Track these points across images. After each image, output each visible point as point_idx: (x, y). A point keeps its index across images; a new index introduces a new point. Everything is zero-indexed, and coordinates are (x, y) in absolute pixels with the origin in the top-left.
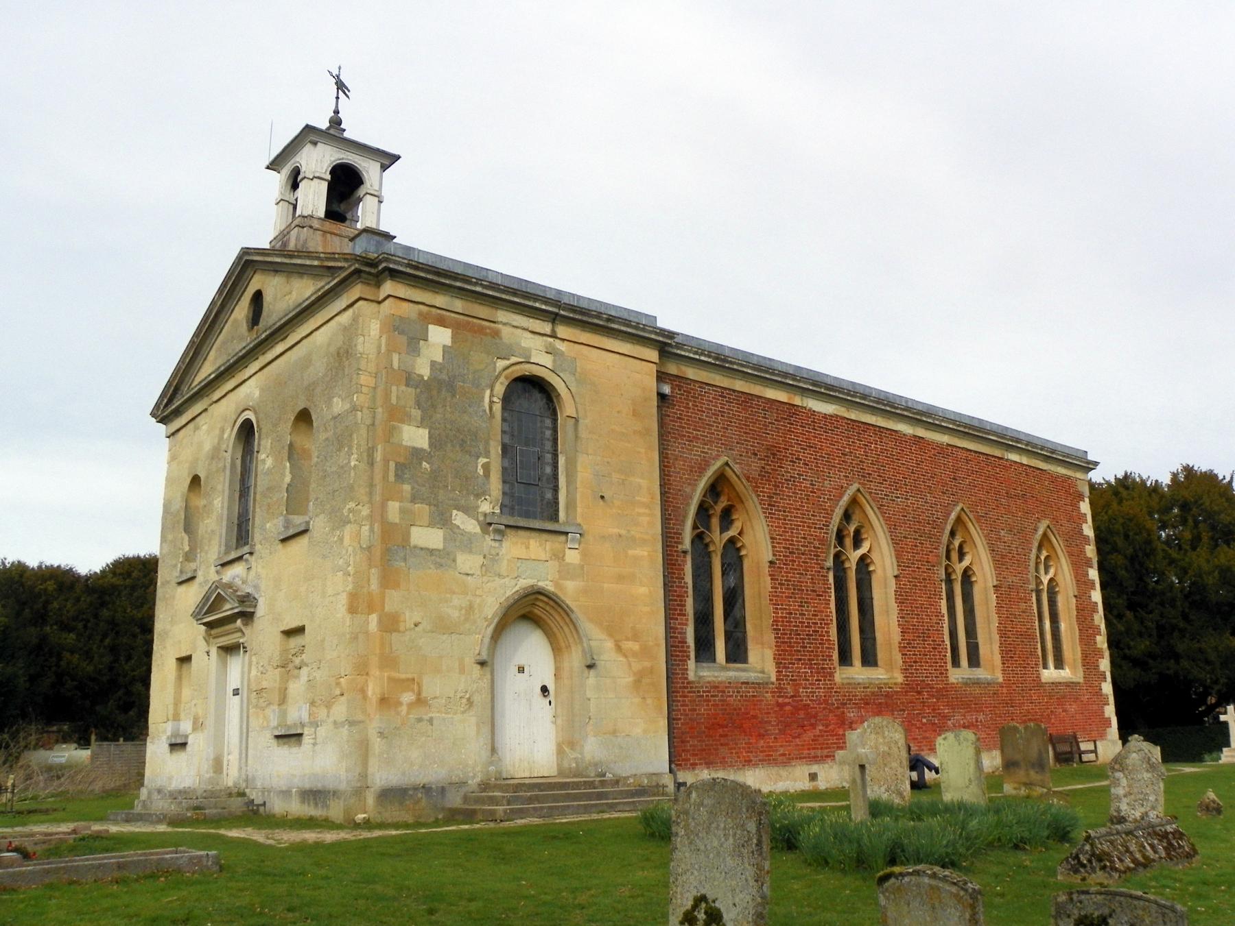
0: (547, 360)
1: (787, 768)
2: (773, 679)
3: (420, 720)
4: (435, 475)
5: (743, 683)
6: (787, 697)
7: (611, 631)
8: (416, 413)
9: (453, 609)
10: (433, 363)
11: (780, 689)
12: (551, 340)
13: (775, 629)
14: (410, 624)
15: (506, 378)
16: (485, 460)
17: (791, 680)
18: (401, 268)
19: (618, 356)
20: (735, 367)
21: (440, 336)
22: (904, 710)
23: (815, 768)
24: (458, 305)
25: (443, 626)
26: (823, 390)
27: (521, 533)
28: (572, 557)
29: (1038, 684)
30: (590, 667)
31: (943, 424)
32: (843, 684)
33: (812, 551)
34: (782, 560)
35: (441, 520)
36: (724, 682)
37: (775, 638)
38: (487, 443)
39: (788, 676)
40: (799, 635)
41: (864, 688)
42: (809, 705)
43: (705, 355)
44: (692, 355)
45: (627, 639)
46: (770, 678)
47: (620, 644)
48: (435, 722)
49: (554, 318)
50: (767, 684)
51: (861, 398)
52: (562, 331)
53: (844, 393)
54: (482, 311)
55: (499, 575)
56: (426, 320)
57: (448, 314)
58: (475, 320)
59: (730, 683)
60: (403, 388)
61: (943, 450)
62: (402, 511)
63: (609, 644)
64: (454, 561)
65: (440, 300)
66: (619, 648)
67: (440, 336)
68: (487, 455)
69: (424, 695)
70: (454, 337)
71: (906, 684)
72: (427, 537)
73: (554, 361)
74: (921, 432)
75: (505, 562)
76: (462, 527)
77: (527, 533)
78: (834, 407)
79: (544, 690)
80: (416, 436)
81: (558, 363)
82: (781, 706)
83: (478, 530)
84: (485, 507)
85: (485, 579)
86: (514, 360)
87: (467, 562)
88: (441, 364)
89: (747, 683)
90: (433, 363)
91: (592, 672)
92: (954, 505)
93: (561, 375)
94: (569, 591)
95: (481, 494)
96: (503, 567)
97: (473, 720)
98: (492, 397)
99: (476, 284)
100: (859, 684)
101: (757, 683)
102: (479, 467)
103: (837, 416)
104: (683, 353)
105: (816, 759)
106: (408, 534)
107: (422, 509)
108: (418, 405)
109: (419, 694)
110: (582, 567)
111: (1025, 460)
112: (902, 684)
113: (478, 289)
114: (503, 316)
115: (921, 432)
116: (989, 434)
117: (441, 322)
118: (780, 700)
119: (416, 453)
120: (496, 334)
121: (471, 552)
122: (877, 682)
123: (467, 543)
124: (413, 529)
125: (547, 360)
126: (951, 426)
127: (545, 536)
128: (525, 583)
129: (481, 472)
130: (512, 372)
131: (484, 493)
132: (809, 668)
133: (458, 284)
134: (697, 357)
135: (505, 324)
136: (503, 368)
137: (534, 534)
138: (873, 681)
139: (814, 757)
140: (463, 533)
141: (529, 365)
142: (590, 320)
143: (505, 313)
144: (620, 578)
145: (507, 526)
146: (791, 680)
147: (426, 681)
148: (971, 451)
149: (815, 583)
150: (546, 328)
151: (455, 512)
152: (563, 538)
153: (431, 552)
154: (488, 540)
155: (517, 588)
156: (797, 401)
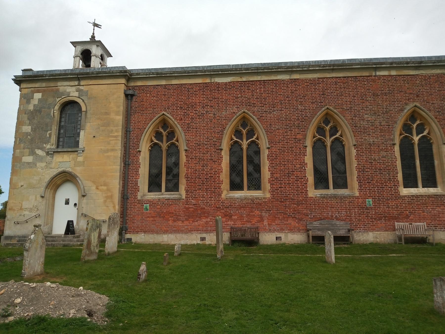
1: (187, 234)
2: (184, 197)
3: (20, 215)
5: (166, 200)
6: (191, 205)
8: (28, 122)
10: (34, 105)
11: (187, 202)
12: (79, 87)
13: (186, 177)
14: (20, 186)
15: (59, 104)
16: (50, 132)
17: (194, 198)
18: (21, 79)
19: (107, 85)
20: (168, 75)
21: (38, 96)
22: (271, 211)
23: (204, 235)
24: (44, 85)
25: (31, 186)
26: (220, 73)
27: (61, 153)
29: (398, 197)
30: (84, 196)
31: (311, 69)
32: (227, 199)
33: (211, 143)
34: (193, 149)
35: (32, 153)
36: (156, 200)
37: (186, 181)
38: (51, 126)
39: (193, 196)
40: (201, 179)
41: (241, 200)
42: (204, 208)
43: (151, 74)
44: (145, 76)
45: (101, 186)
46: (182, 197)
47: (98, 187)
48: (25, 216)
49: (79, 79)
50: (180, 199)
51: (245, 70)
52: (82, 83)
53: (233, 71)
54: (52, 84)
55: (51, 168)
56: (33, 92)
57: (41, 88)
58: (50, 88)
59: (159, 200)
60: (24, 115)
61: (313, 82)
64: (36, 165)
65: (37, 85)
67: (38, 96)
68: (51, 130)
70: (42, 96)
71: (272, 198)
72: (28, 159)
73: (79, 94)
74: (296, 76)
75: (54, 163)
76: (39, 154)
77: (63, 153)
80: (27, 129)
81: (81, 94)
83: (45, 154)
84: (48, 146)
85: (46, 170)
86: (63, 97)
88: (37, 105)
89: (169, 200)
90: (34, 105)
91: (85, 198)
92: (321, 108)
93: (82, 98)
94: (78, 171)
95: (47, 142)
96: (53, 165)
98: (56, 111)
99: (46, 76)
100: (238, 198)
101: (174, 200)
102: (48, 134)
103: (234, 82)
104: (141, 76)
106: (21, 159)
108: (28, 119)
109: (21, 207)
111: (394, 73)
112: (269, 198)
113: (47, 78)
114: (59, 84)
115: (296, 76)
116: (352, 66)
117: (38, 92)
118: (187, 206)
119: (27, 134)
120: (58, 90)
121: (42, 162)
122: (250, 197)
123: (41, 159)
124: (23, 158)
125: (77, 94)
126: (317, 68)
127: (70, 153)
128: (60, 170)
129: (48, 136)
130: (62, 101)
131: (49, 142)
132: (205, 192)
133: (40, 78)
134: (148, 76)
135: (61, 86)
136: (59, 101)
137: (65, 153)
138: (248, 197)
139: (205, 230)
140: (40, 156)
141: (69, 97)
142: (90, 76)
143: (60, 82)
145: (54, 152)
146: (194, 198)
148: (340, 77)
149: (213, 156)
150: (76, 83)
151: (36, 150)
152: (76, 153)
153: (28, 163)
154: (49, 158)
155: (58, 172)
156: (208, 81)
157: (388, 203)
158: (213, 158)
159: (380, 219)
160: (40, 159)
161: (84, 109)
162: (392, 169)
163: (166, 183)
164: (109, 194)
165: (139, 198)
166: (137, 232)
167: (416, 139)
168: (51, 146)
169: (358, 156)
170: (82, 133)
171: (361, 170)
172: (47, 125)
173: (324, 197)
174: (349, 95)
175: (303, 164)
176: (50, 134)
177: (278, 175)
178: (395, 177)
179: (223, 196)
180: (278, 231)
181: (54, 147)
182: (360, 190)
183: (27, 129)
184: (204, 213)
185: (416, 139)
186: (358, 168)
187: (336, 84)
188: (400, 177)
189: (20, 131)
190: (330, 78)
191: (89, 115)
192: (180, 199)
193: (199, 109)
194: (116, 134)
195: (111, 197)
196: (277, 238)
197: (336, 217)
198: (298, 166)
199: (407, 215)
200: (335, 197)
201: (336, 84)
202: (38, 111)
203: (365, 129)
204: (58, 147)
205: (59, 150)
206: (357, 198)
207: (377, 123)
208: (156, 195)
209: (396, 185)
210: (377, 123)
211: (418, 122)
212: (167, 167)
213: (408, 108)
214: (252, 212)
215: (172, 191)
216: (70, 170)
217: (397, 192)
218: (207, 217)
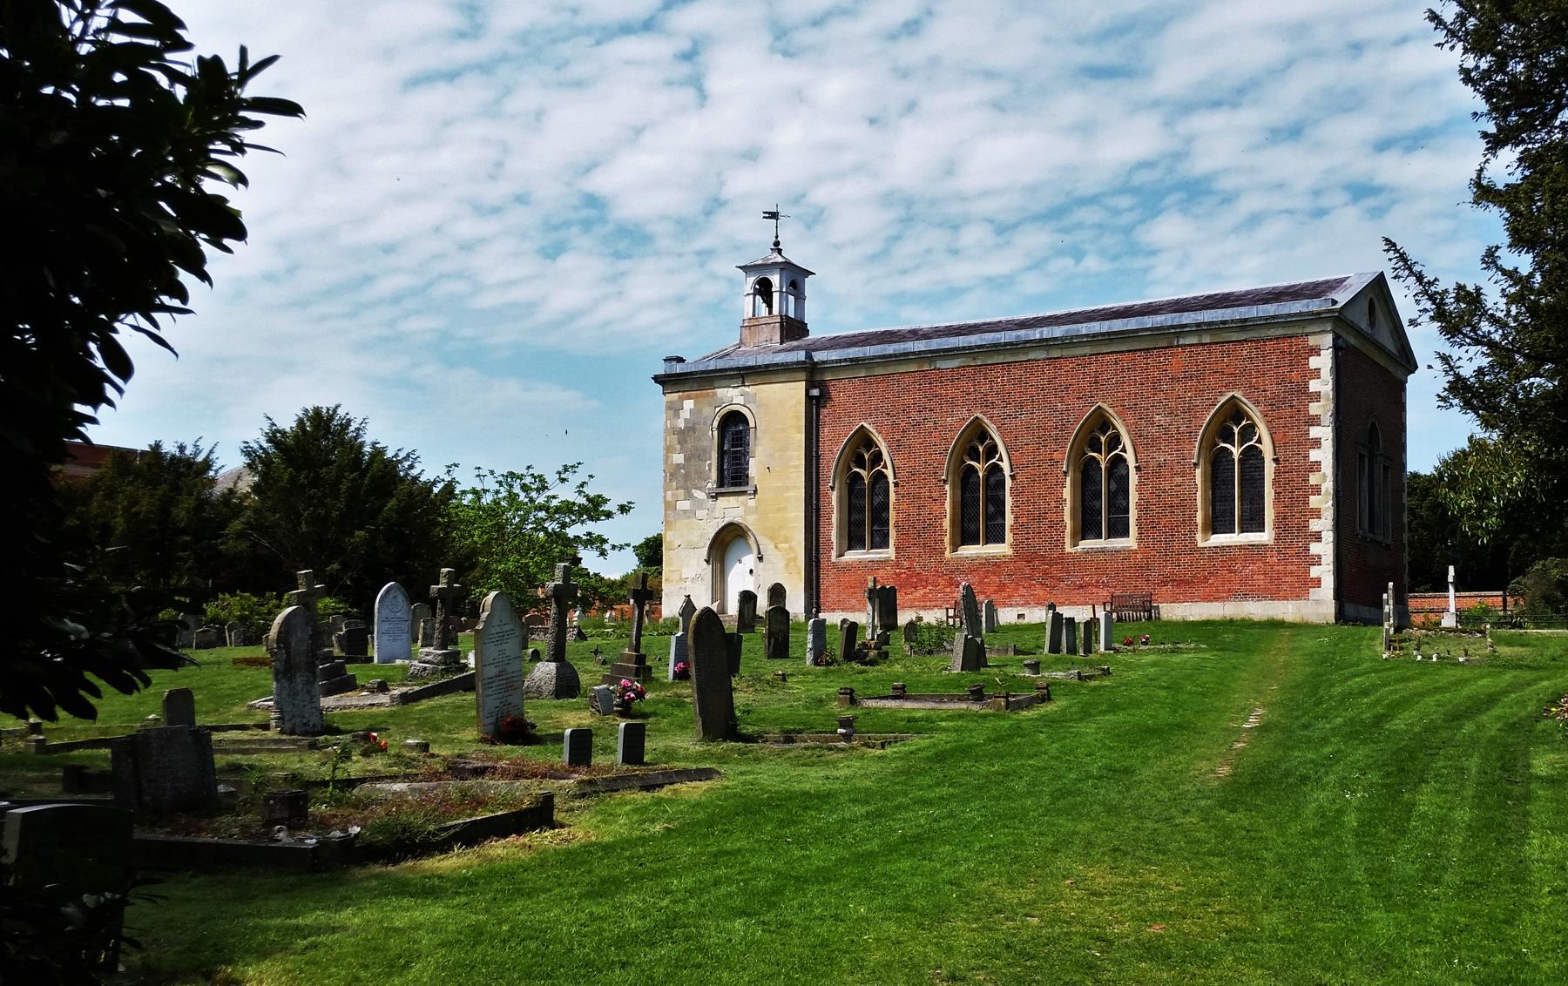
0: (741, 400)
2: (893, 558)
4: (687, 475)
7: (771, 538)
8: (678, 447)
9: (694, 538)
10: (685, 419)
11: (898, 565)
21: (689, 404)
28: (752, 503)
35: (689, 496)
62: (673, 495)
63: (772, 546)
66: (776, 547)
69: (684, 576)
72: (684, 505)
78: (960, 360)
79: (751, 571)
80: (679, 458)
82: (898, 575)
84: (709, 485)
87: (701, 513)
90: (685, 419)
94: (749, 522)
97: (704, 587)
105: (924, 608)
107: (681, 491)
108: (679, 443)
110: (757, 507)
125: (741, 400)
128: (727, 520)
144: (779, 510)
147: (683, 571)
151: (693, 491)
153: (685, 511)
157: (1178, 559)
158: (934, 495)
159: (1165, 583)
160: (698, 504)
161: (752, 424)
162: (1187, 506)
163: (872, 536)
164: (792, 555)
165: (833, 559)
166: (833, 610)
167: (1236, 452)
168: (711, 484)
169: (1141, 484)
170: (752, 462)
171: (1143, 507)
172: (704, 450)
173: (1088, 552)
174: (1135, 381)
175: (1061, 501)
176: (710, 465)
177: (1025, 520)
178: (1193, 517)
179: (947, 554)
180: (1022, 605)
181: (715, 486)
182: (1140, 540)
183: (679, 458)
184: (921, 580)
185: (1236, 452)
186: (1138, 505)
187: (1116, 363)
188: (1199, 518)
189: (669, 462)
190: (1107, 353)
191: (759, 434)
192: (886, 561)
193: (914, 414)
194: (797, 463)
195: (795, 559)
196: (1020, 616)
197: (1103, 582)
198: (1053, 504)
199: (1205, 578)
200: (1103, 551)
201: (1116, 363)
202: (691, 428)
203: (1153, 440)
204: (721, 483)
205: (723, 490)
206: (1135, 552)
207: (1173, 429)
208: (855, 554)
209: (1193, 532)
210: (1173, 429)
211: (1244, 423)
212: (873, 510)
213: (1223, 400)
214: (986, 577)
215: (881, 548)
216: (738, 520)
217: (1194, 542)
218: (925, 587)
